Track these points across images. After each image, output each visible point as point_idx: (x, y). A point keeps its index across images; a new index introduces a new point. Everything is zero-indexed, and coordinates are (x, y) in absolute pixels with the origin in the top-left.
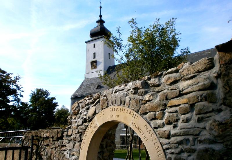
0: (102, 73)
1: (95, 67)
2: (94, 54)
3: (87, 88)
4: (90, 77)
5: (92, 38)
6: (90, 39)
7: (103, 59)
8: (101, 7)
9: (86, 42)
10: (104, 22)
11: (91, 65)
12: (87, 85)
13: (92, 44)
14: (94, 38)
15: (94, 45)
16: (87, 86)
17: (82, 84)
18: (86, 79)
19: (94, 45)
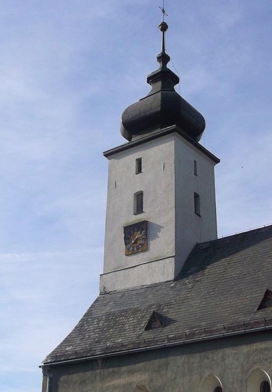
0: (166, 271)
1: (142, 245)
2: (139, 197)
3: (109, 327)
4: (120, 287)
5: (129, 139)
6: (124, 141)
7: (172, 214)
8: (164, 27)
9: (109, 154)
10: (176, 80)
11: (126, 239)
12: (108, 315)
13: (130, 159)
14: (135, 139)
15: (139, 162)
16: (107, 320)
17: (89, 314)
18: (104, 293)
19: (139, 162)
